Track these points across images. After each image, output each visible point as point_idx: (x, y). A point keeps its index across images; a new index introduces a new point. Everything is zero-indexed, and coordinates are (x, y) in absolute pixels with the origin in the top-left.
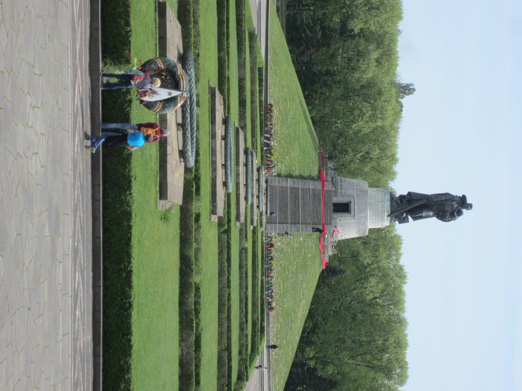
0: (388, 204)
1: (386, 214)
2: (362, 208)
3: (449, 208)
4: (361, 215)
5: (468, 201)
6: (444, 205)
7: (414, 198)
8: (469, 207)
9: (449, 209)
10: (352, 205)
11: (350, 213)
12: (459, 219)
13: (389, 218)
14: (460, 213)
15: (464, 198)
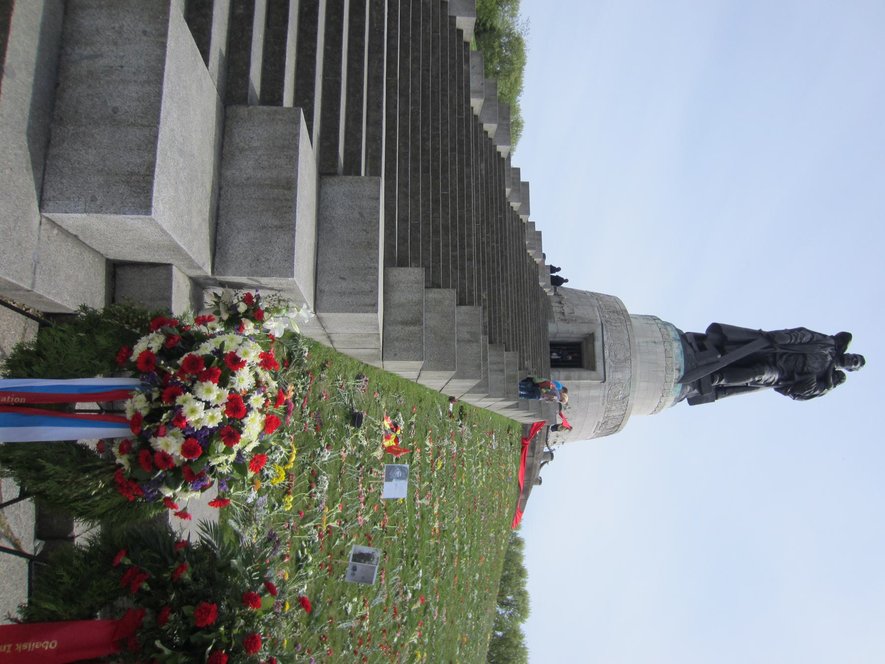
0: (677, 348)
1: (676, 375)
2: (620, 356)
3: (815, 366)
4: (619, 375)
5: (851, 349)
6: (804, 356)
7: (731, 337)
8: (857, 360)
9: (816, 365)
10: (598, 344)
11: (593, 368)
12: (834, 394)
13: (680, 385)
14: (840, 378)
15: (844, 338)
